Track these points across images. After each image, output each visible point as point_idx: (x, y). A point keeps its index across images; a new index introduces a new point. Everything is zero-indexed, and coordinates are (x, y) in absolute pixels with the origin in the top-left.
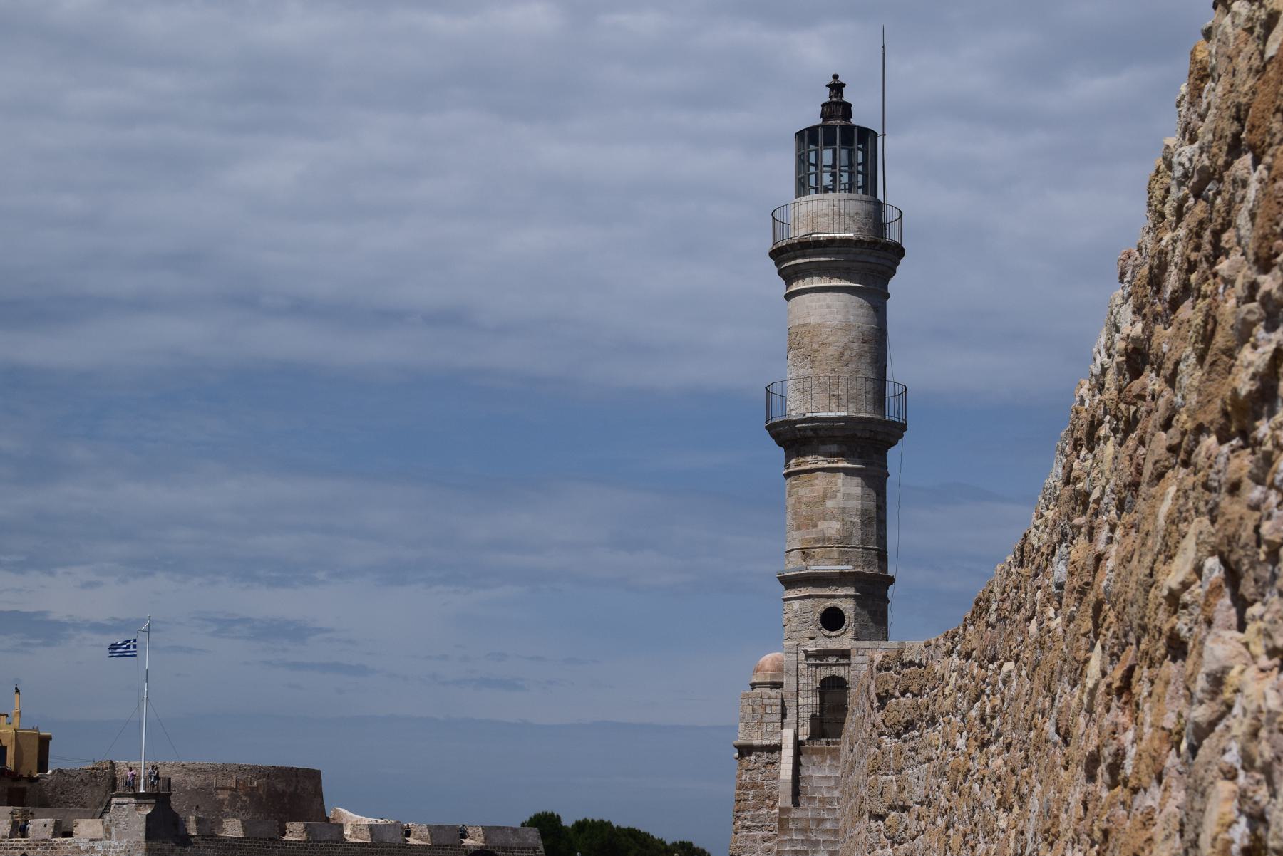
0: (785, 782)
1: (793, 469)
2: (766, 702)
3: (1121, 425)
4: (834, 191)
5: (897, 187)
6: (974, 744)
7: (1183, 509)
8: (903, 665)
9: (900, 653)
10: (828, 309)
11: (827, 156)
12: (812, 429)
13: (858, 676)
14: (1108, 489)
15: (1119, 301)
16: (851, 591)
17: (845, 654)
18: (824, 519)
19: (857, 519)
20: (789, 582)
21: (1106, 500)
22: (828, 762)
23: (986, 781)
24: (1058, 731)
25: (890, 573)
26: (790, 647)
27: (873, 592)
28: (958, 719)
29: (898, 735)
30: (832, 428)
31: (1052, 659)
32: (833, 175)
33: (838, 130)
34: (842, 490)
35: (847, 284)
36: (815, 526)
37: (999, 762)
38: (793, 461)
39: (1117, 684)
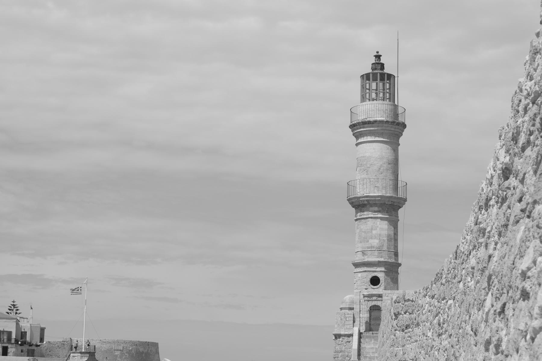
0: (354, 350)
1: (358, 217)
2: (347, 316)
3: (500, 200)
4: (376, 100)
5: (403, 98)
6: (435, 335)
7: (528, 236)
8: (405, 301)
9: (404, 296)
10: (374, 150)
11: (374, 86)
13: (385, 306)
14: (494, 227)
15: (499, 147)
17: (380, 296)
18: (372, 239)
19: (385, 239)
20: (357, 265)
21: (493, 232)
22: (373, 341)
23: (441, 350)
24: (472, 330)
25: (399, 262)
26: (357, 293)
27: (393, 269)
28: (429, 324)
29: (403, 331)
30: (375, 200)
31: (470, 299)
32: (376, 93)
33: (378, 74)
34: (379, 226)
35: (382, 139)
36: (368, 241)
37: (446, 342)
38: (359, 214)
39: (498, 310)
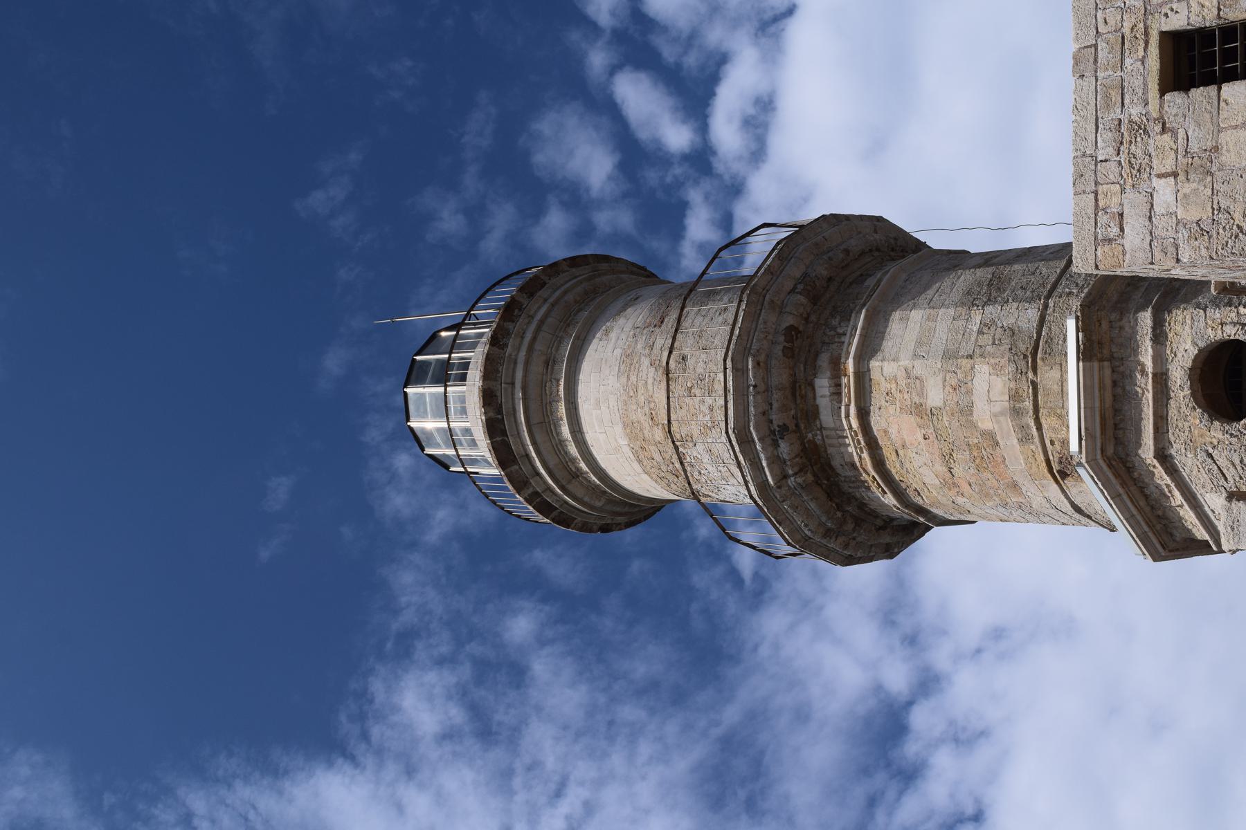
12: (773, 437)
16: (1146, 319)
18: (967, 411)
19: (977, 316)
30: (765, 390)
34: (905, 362)
36: (990, 437)
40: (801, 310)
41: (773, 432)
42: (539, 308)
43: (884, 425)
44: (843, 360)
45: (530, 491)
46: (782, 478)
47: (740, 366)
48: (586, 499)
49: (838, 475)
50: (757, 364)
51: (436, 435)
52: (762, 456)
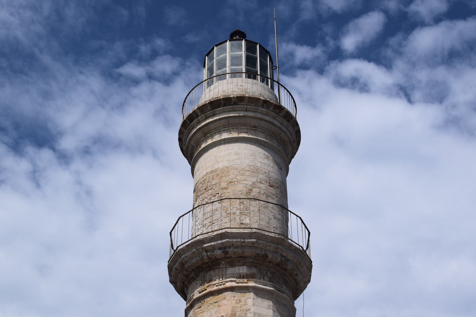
12: (223, 248)
30: (242, 246)
34: (253, 309)
40: (274, 260)
41: (225, 248)
42: (279, 121)
43: (228, 298)
44: (254, 280)
45: (199, 113)
46: (206, 250)
47: (253, 235)
48: (194, 138)
49: (207, 272)
50: (253, 243)
51: (224, 69)
52: (215, 243)
